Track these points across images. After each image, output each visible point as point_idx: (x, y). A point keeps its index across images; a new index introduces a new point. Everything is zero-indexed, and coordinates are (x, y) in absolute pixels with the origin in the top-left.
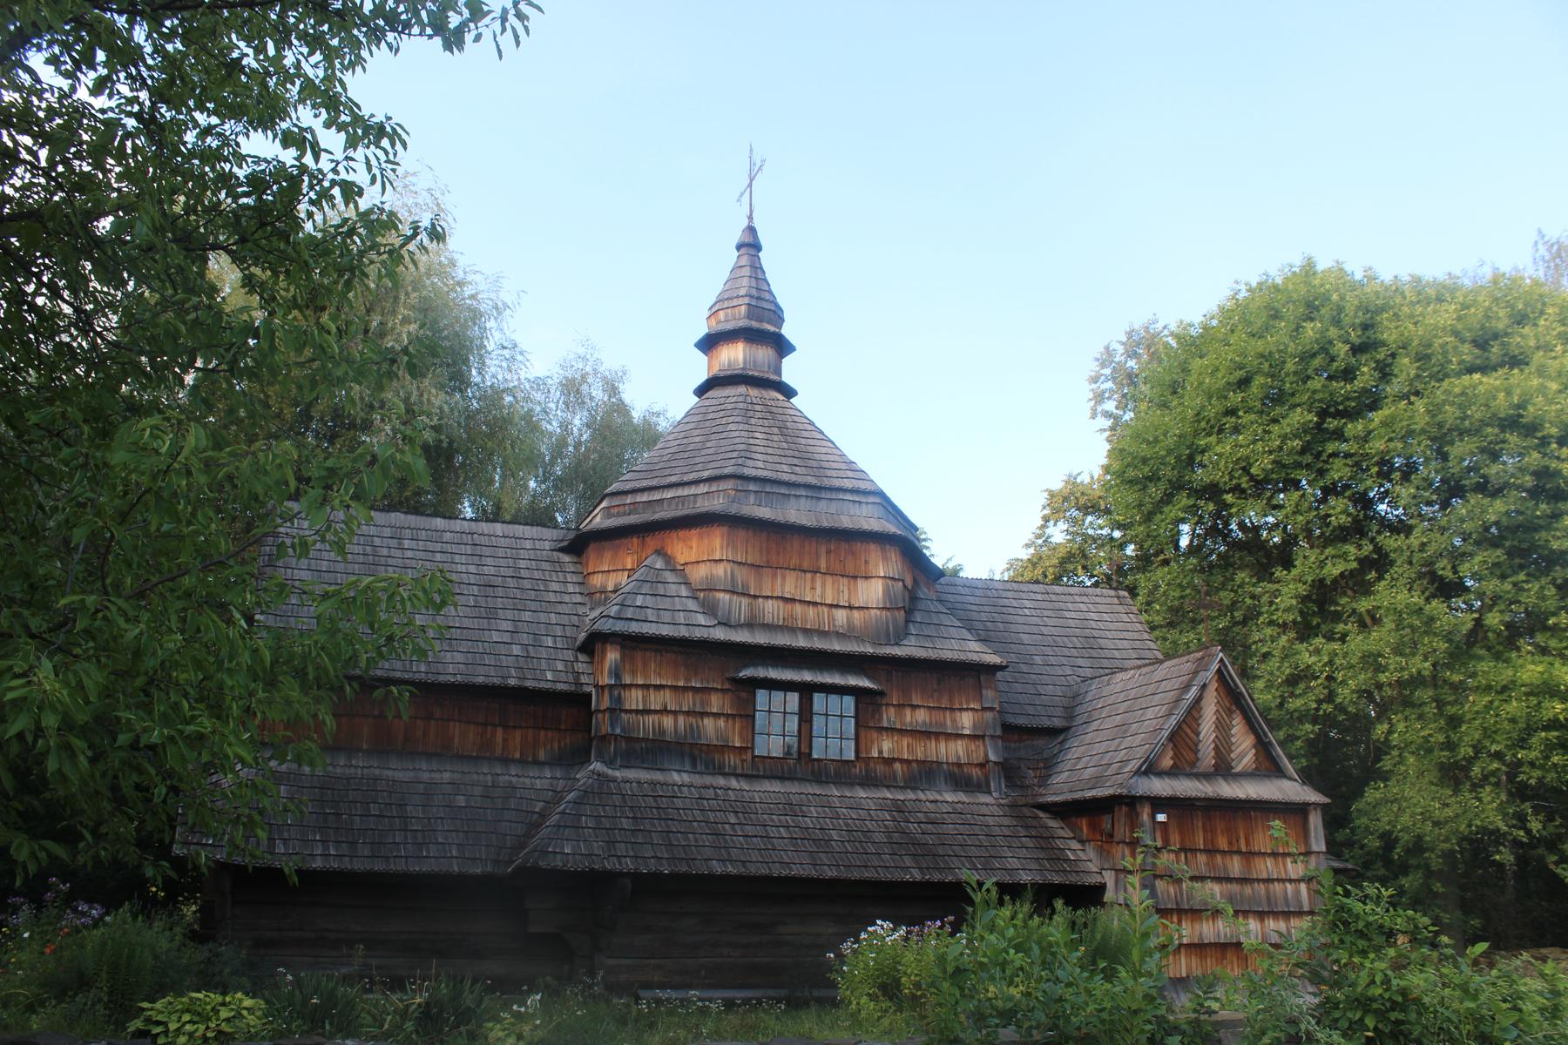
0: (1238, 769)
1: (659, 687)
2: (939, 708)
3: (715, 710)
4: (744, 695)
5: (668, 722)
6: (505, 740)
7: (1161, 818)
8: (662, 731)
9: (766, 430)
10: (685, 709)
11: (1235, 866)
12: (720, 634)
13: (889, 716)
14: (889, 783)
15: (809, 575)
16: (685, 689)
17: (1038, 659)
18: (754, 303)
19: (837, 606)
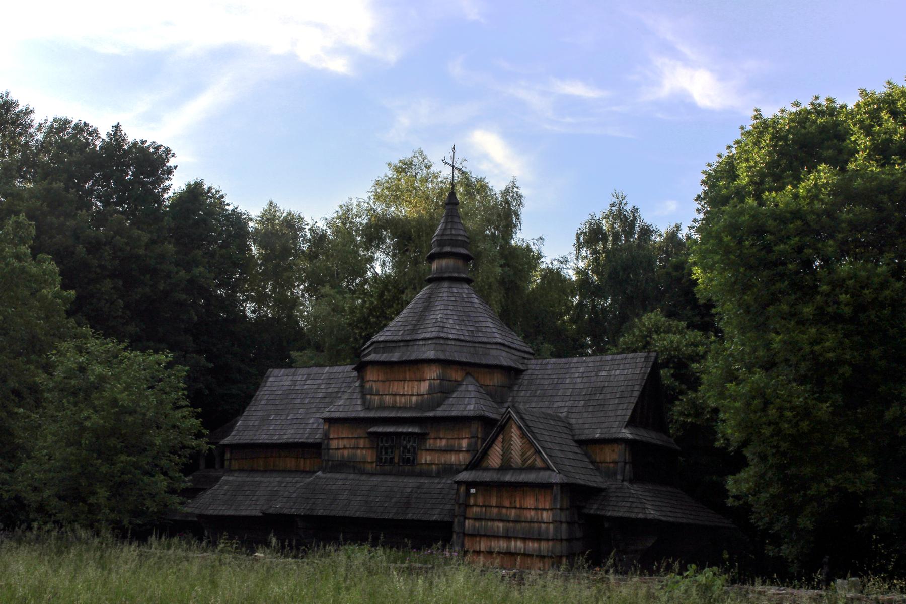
1: (343, 438)
2: (452, 439)
3: (362, 447)
5: (346, 453)
6: (304, 463)
7: (472, 491)
8: (343, 456)
10: (352, 447)
11: (513, 513)
12: (362, 415)
13: (430, 443)
14: (428, 474)
15: (403, 382)
16: (352, 438)
19: (413, 395)
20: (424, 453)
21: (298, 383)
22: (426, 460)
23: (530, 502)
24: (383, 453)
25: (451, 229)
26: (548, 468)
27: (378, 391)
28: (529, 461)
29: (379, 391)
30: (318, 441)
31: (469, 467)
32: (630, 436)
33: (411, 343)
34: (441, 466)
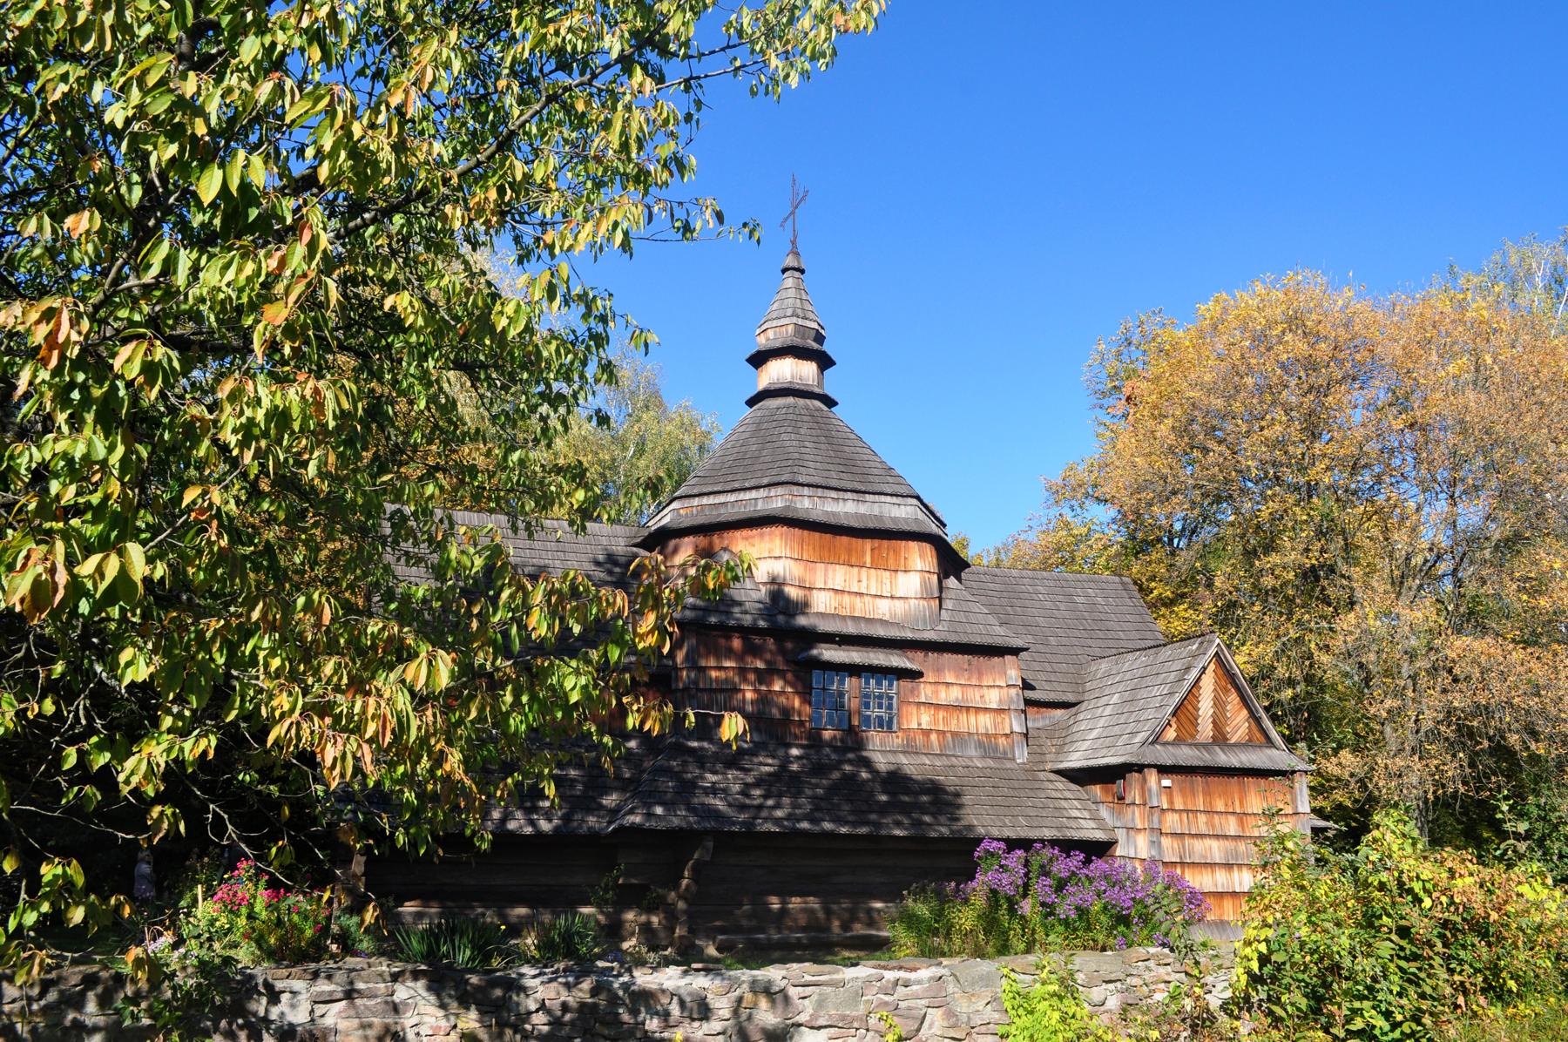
0: (1233, 741)
7: (1166, 782)
9: (815, 439)
17: (1052, 640)
20: (913, 709)
22: (919, 724)
23: (1255, 804)
26: (1270, 742)
28: (1239, 732)
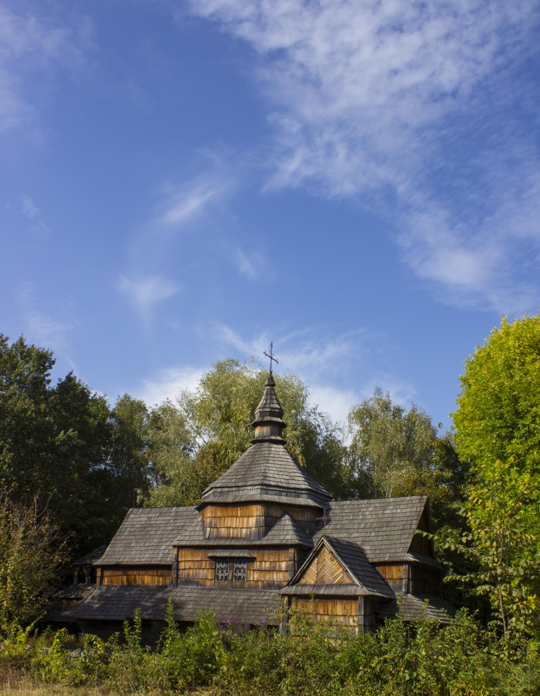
3: (204, 567)
4: (213, 562)
5: (191, 572)
12: (204, 543)
13: (257, 565)
18: (261, 410)
19: (243, 528)
21: (153, 519)
22: (253, 578)
24: (220, 572)
25: (270, 403)
26: (353, 584)
27: (216, 524)
28: (338, 579)
29: (217, 525)
30: (169, 563)
31: (291, 583)
32: (412, 559)
33: (242, 488)
34: (265, 582)
